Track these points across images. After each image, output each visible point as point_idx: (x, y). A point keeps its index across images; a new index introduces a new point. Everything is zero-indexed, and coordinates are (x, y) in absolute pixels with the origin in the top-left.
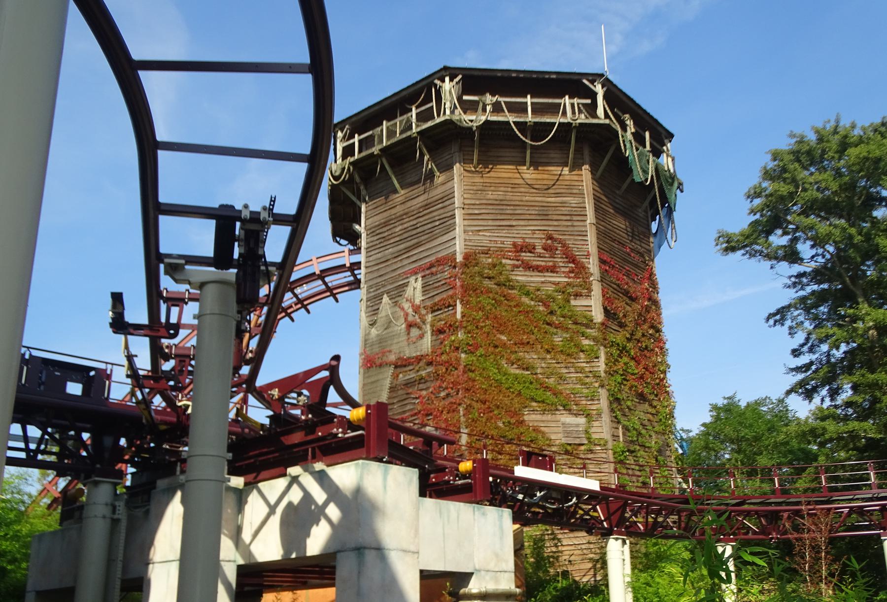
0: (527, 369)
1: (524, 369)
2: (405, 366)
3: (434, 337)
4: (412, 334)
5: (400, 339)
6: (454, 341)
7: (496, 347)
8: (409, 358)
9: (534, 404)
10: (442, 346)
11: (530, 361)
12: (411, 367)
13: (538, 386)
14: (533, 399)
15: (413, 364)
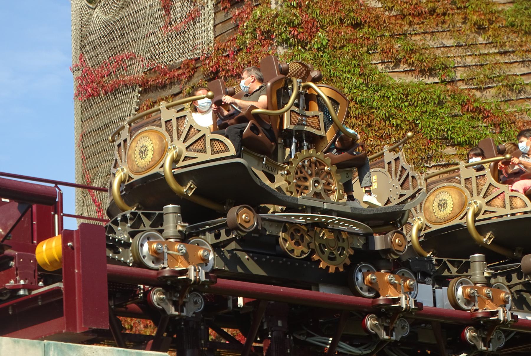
0: (431, 72)
1: (423, 72)
2: (164, 87)
3: (221, 17)
4: (175, 14)
5: (152, 28)
6: (259, 20)
7: (357, 26)
8: (171, 68)
9: (450, 150)
10: (238, 35)
11: (438, 52)
12: (176, 89)
13: (457, 110)
14: (447, 141)
15: (179, 82)
